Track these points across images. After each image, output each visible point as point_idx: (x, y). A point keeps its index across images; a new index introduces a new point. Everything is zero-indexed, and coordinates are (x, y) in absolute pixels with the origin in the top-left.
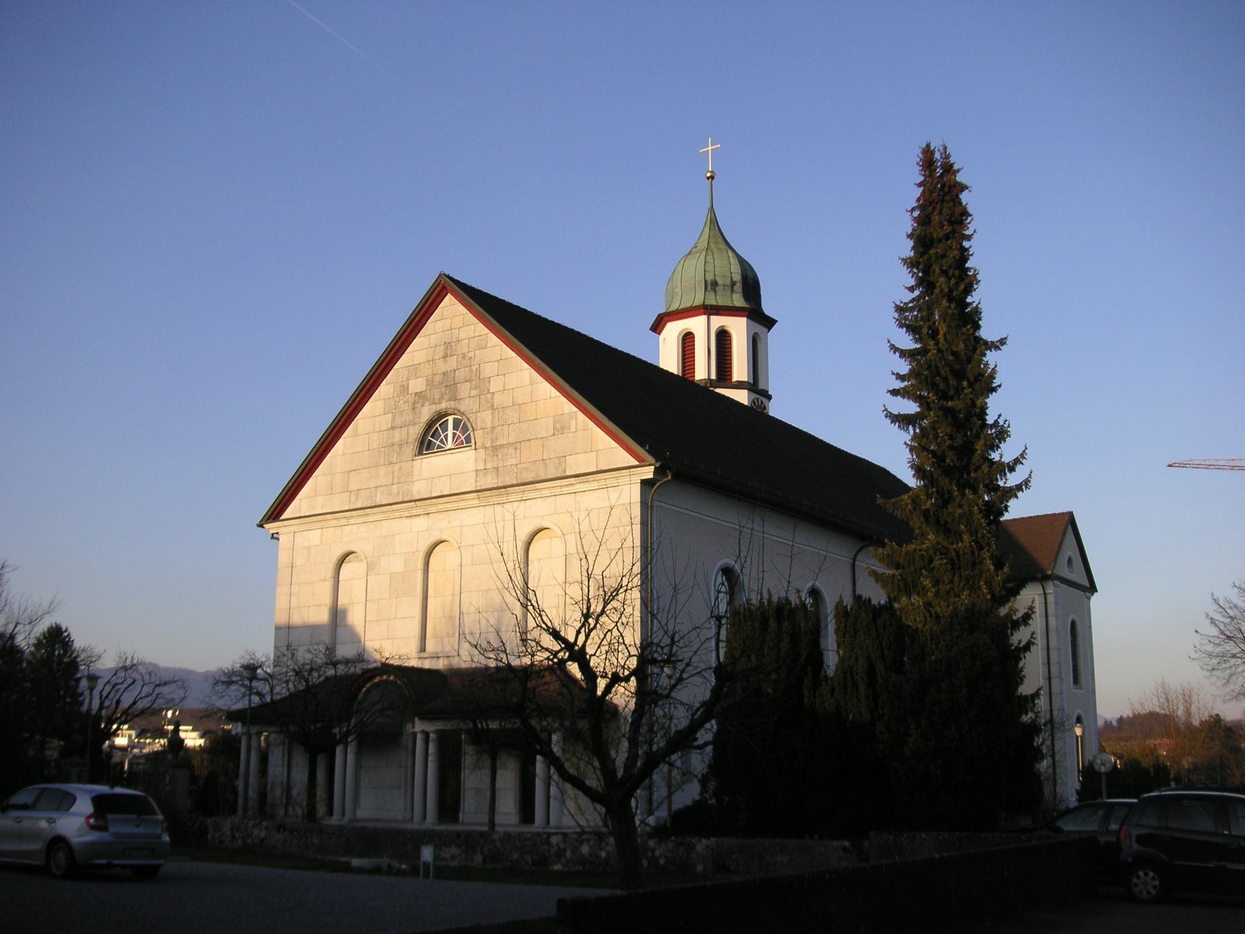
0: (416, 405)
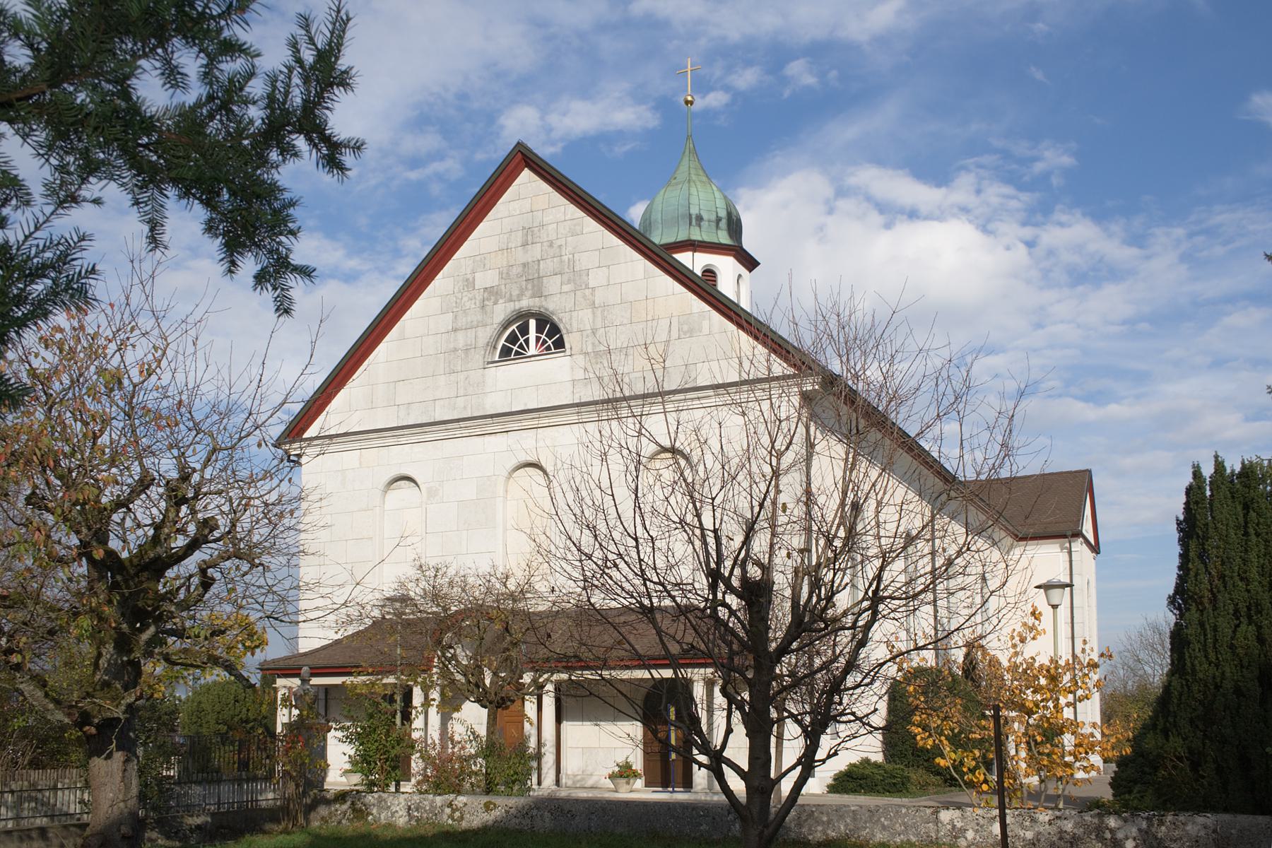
0: (486, 303)
